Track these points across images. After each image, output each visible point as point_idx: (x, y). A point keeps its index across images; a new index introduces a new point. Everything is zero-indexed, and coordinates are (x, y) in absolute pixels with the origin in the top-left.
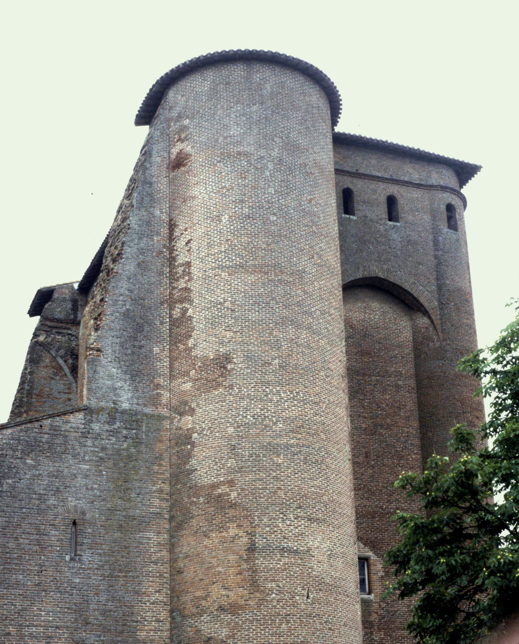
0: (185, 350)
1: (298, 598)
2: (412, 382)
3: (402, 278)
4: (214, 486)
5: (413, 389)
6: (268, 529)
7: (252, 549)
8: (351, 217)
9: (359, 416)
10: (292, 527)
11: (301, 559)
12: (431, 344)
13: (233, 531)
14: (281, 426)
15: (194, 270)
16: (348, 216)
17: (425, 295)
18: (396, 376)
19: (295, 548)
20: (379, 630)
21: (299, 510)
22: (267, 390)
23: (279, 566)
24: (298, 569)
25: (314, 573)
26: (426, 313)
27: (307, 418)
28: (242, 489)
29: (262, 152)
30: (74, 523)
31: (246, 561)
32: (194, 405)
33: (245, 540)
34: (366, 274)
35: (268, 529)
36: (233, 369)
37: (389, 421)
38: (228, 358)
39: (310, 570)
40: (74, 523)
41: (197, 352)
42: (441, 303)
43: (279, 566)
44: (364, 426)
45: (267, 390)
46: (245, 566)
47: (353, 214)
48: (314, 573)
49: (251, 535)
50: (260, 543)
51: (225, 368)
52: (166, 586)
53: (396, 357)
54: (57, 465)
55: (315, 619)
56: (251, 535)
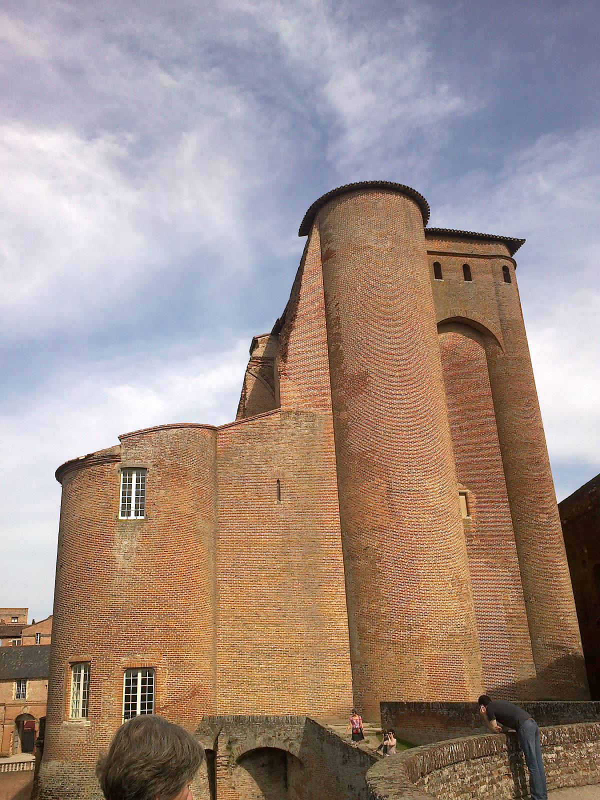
0: (340, 371)
1: (421, 520)
2: (488, 381)
3: (476, 316)
4: (364, 454)
5: (488, 385)
6: (399, 478)
8: (440, 280)
10: (414, 476)
12: (498, 356)
13: (378, 480)
14: (403, 414)
15: (342, 322)
16: (438, 280)
17: (491, 324)
19: (417, 489)
21: (418, 465)
22: (393, 392)
23: (408, 501)
24: (420, 502)
25: (431, 504)
26: (493, 336)
27: (419, 408)
29: (380, 245)
30: (278, 481)
31: (387, 499)
32: (347, 404)
35: (399, 478)
36: (370, 381)
37: (473, 406)
38: (366, 374)
39: (428, 502)
40: (278, 481)
41: (347, 372)
42: (502, 330)
43: (408, 501)
45: (393, 392)
47: (442, 279)
48: (431, 504)
50: (395, 487)
51: (365, 380)
53: (475, 365)
54: (265, 446)
55: (434, 533)
56: (389, 483)
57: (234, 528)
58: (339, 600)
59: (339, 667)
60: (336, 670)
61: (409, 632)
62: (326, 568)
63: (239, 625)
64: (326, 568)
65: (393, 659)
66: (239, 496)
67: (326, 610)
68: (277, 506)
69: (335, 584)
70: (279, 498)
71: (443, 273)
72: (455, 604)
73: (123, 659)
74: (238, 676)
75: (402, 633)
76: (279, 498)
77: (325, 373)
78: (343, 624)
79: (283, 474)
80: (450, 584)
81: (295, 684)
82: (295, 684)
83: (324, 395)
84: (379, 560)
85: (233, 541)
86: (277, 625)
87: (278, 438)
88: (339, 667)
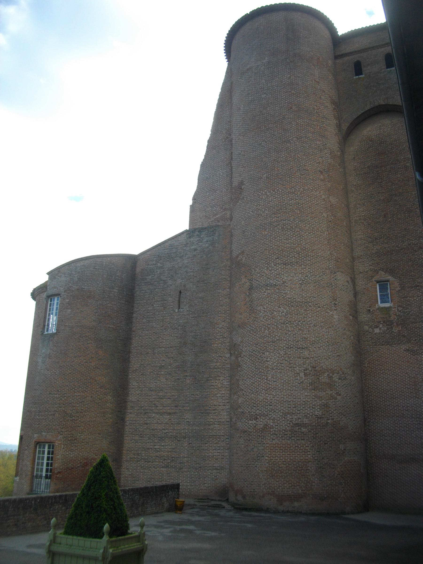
1: (275, 313)
7: (251, 288)
8: (360, 76)
9: (379, 193)
10: (273, 271)
11: (278, 289)
13: (244, 280)
14: (267, 212)
16: (357, 77)
18: (404, 161)
19: (274, 283)
20: (398, 325)
21: (277, 260)
22: (260, 194)
23: (264, 296)
24: (276, 296)
25: (287, 296)
27: (284, 203)
28: (247, 255)
30: (180, 292)
33: (248, 284)
34: (372, 106)
35: (259, 275)
37: (401, 191)
39: (284, 295)
40: (180, 292)
43: (264, 296)
44: (382, 198)
45: (260, 194)
46: (248, 299)
47: (362, 74)
48: (287, 296)
49: (251, 280)
51: (241, 188)
52: (228, 317)
54: (172, 263)
55: (287, 324)
57: (144, 335)
58: (223, 392)
59: (219, 451)
60: (216, 454)
61: (255, 422)
62: (214, 364)
63: (141, 413)
64: (214, 364)
65: (243, 446)
66: (149, 309)
67: (212, 402)
68: (178, 314)
69: (221, 378)
70: (179, 308)
71: (363, 69)
72: (306, 394)
73: (36, 435)
74: (138, 454)
75: (250, 422)
76: (179, 308)
77: (227, 190)
78: (225, 414)
79: (185, 286)
80: (302, 374)
81: (180, 463)
82: (180, 463)
83: (225, 209)
84: (241, 353)
85: (142, 346)
86: (170, 414)
87: (183, 256)
88: (219, 451)
